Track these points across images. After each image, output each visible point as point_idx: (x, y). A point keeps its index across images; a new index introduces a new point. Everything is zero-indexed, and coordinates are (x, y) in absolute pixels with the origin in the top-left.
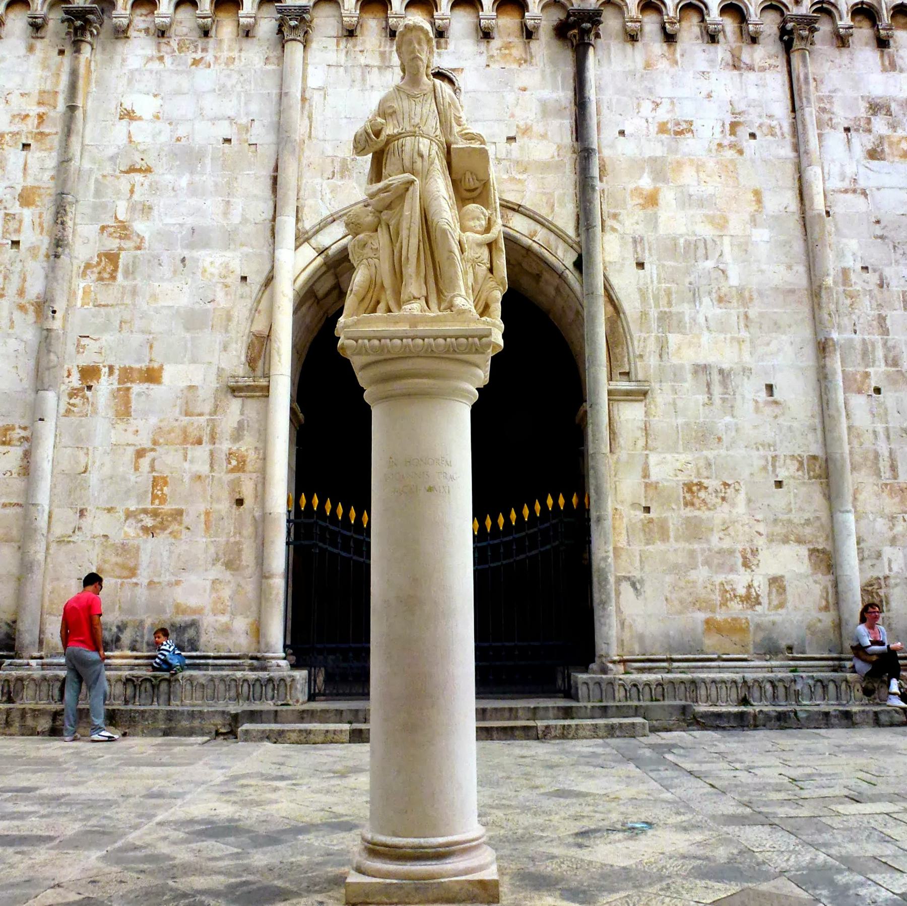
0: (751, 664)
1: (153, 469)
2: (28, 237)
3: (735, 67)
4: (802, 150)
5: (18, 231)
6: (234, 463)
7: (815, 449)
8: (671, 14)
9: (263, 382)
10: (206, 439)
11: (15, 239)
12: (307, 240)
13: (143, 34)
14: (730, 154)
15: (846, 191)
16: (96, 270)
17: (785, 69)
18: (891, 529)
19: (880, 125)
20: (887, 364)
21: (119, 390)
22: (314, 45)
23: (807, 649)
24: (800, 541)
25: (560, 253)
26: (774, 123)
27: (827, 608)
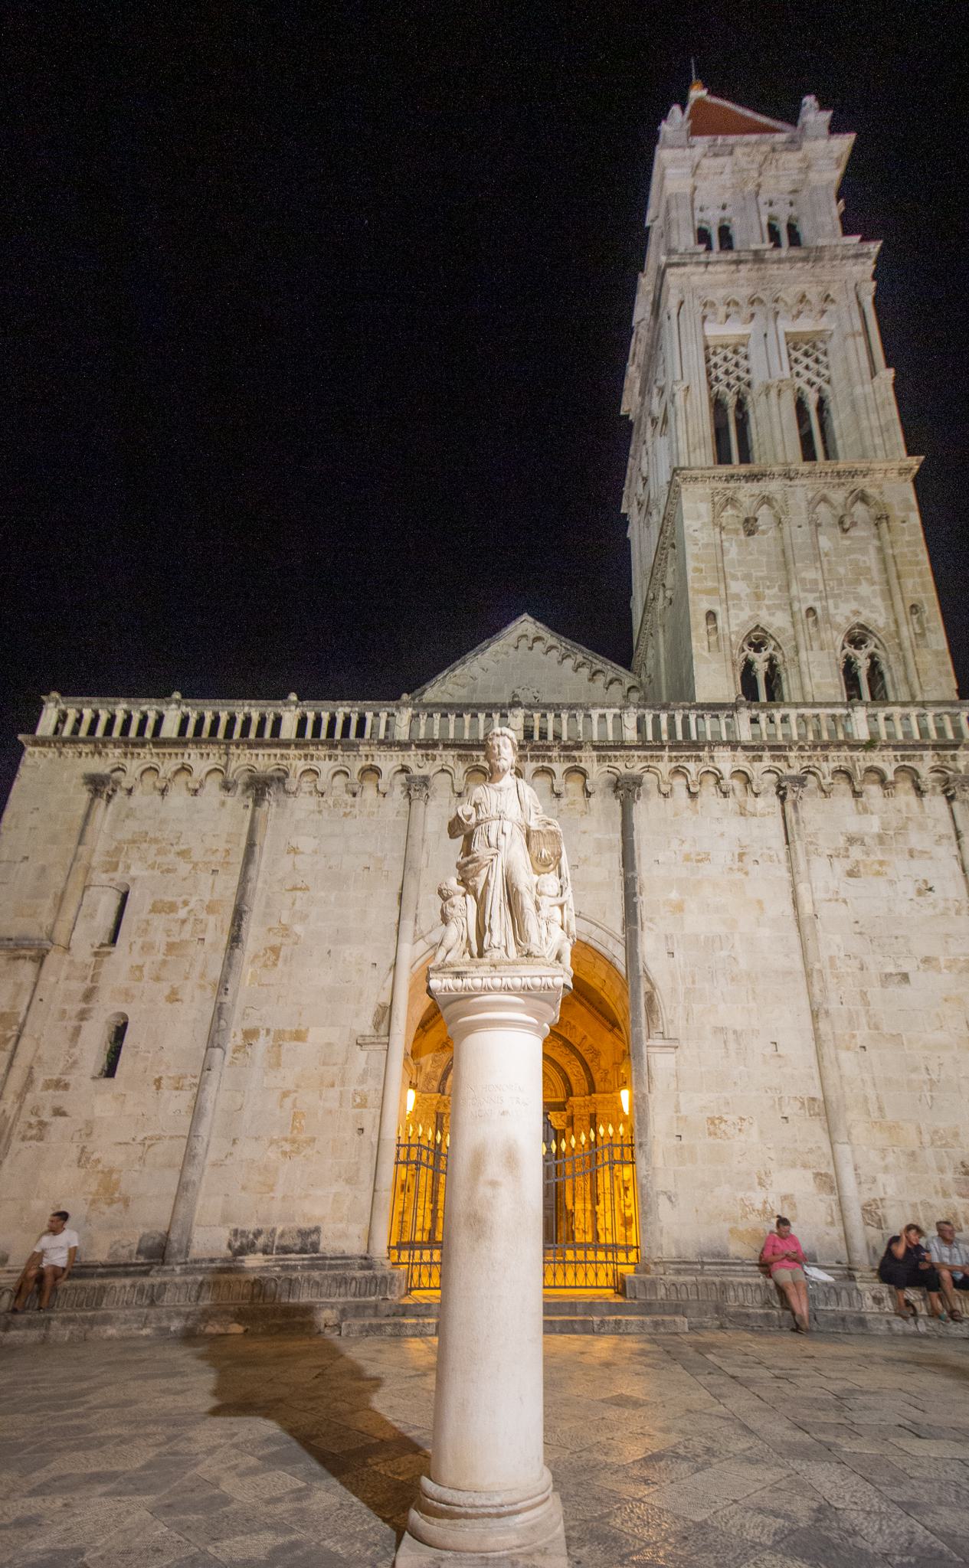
1: (294, 1106)
3: (741, 814)
4: (795, 870)
6: (358, 1100)
8: (694, 778)
9: (385, 1040)
10: (337, 1083)
12: (423, 937)
14: (739, 876)
15: (830, 900)
18: (883, 1159)
19: (856, 852)
20: (870, 1028)
21: (273, 1046)
22: (432, 803)
23: (818, 1258)
24: (805, 1166)
25: (610, 947)
26: (772, 853)
27: (832, 1223)
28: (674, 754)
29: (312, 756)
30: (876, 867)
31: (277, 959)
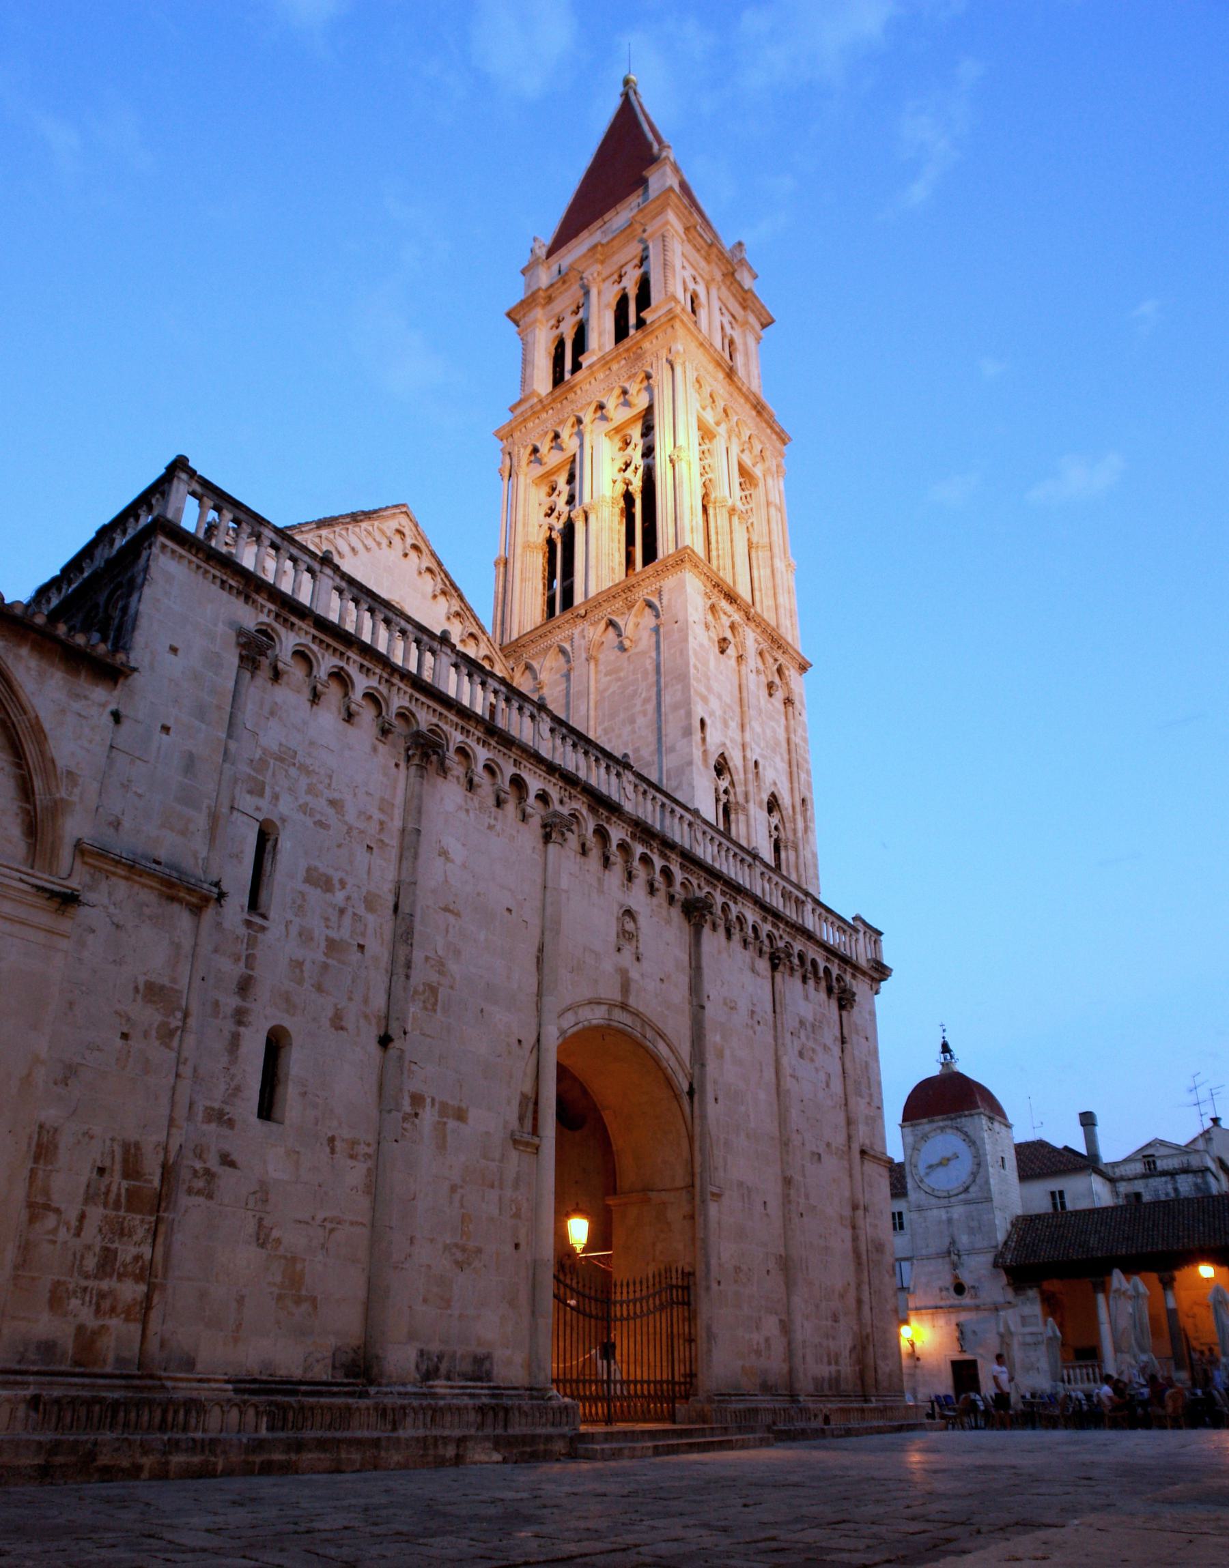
0: (759, 1398)
2: (373, 946)
5: (363, 934)
7: (782, 1251)
11: (362, 943)
13: (455, 780)
16: (422, 998)
17: (770, 980)
24: (776, 1314)
25: (681, 1079)
28: (724, 888)
29: (468, 731)
30: (811, 1052)
31: (435, 1003)
